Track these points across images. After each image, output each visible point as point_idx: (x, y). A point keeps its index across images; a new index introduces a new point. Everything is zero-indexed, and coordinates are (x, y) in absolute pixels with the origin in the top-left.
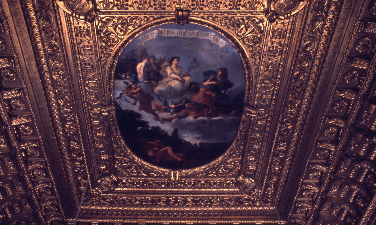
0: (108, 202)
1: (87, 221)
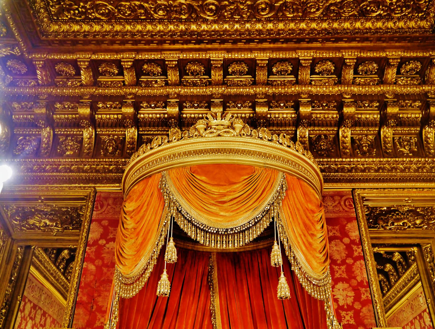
0: (102, 14)
1: (70, 57)
